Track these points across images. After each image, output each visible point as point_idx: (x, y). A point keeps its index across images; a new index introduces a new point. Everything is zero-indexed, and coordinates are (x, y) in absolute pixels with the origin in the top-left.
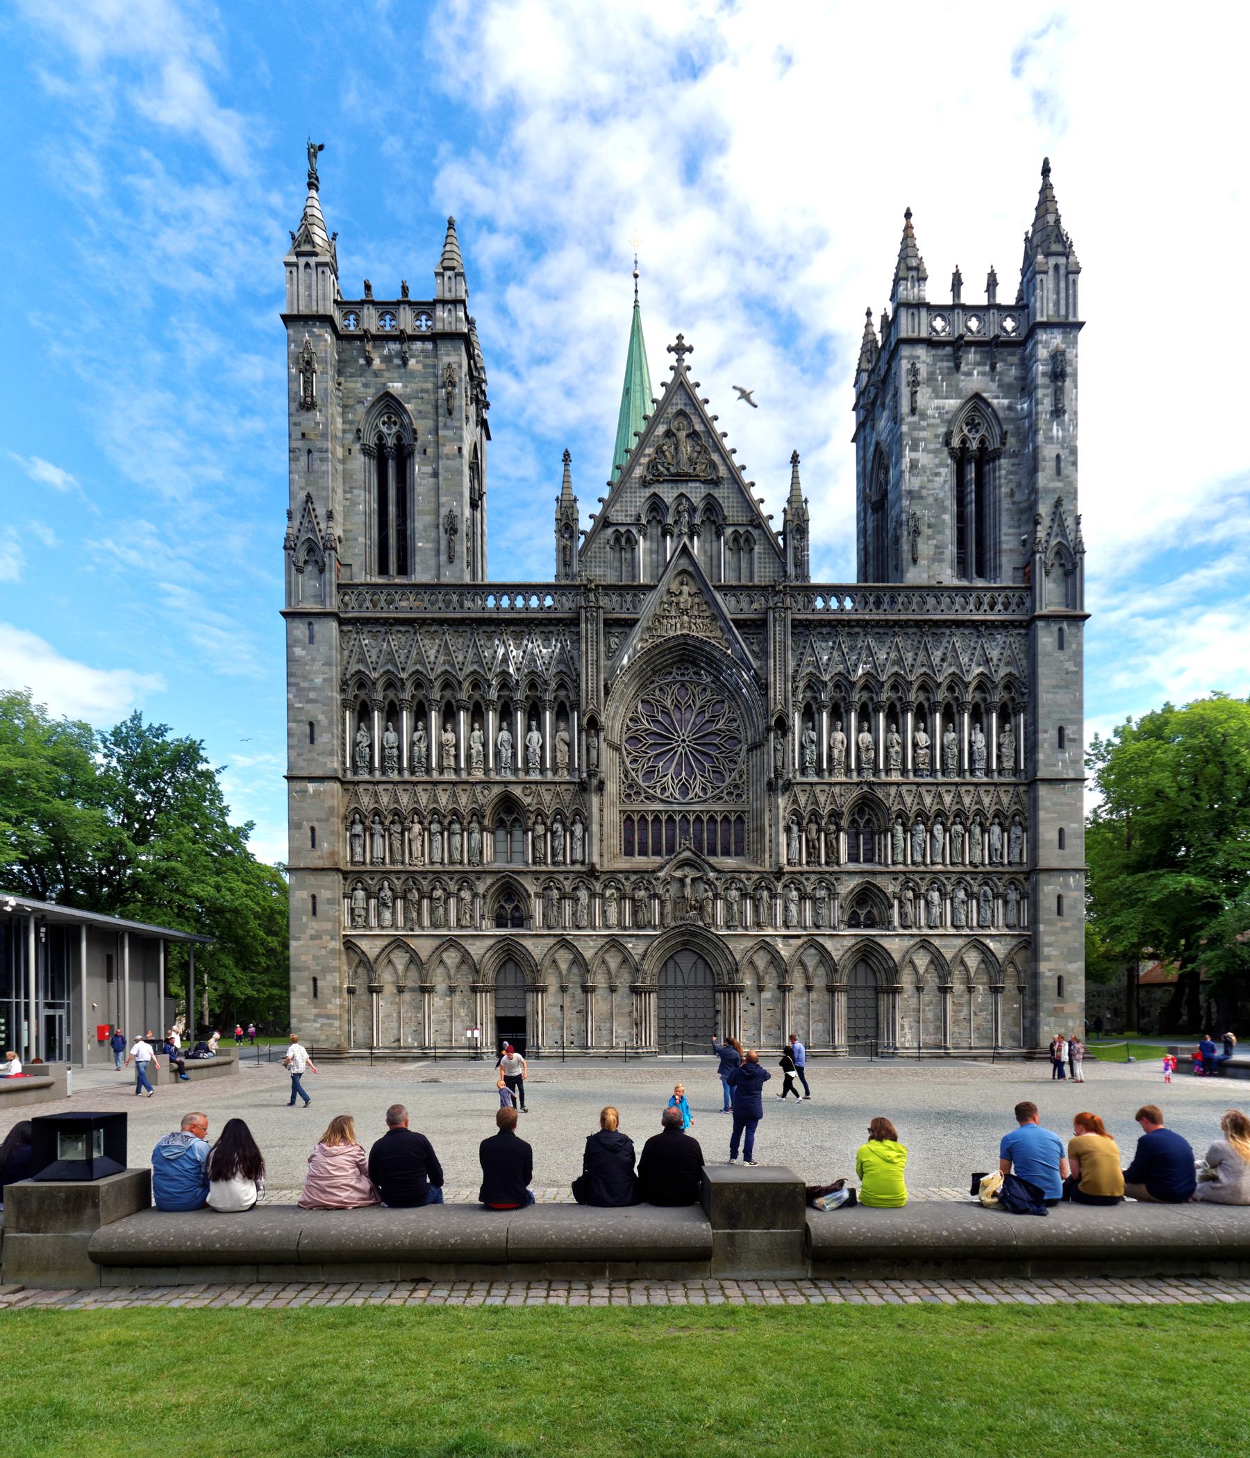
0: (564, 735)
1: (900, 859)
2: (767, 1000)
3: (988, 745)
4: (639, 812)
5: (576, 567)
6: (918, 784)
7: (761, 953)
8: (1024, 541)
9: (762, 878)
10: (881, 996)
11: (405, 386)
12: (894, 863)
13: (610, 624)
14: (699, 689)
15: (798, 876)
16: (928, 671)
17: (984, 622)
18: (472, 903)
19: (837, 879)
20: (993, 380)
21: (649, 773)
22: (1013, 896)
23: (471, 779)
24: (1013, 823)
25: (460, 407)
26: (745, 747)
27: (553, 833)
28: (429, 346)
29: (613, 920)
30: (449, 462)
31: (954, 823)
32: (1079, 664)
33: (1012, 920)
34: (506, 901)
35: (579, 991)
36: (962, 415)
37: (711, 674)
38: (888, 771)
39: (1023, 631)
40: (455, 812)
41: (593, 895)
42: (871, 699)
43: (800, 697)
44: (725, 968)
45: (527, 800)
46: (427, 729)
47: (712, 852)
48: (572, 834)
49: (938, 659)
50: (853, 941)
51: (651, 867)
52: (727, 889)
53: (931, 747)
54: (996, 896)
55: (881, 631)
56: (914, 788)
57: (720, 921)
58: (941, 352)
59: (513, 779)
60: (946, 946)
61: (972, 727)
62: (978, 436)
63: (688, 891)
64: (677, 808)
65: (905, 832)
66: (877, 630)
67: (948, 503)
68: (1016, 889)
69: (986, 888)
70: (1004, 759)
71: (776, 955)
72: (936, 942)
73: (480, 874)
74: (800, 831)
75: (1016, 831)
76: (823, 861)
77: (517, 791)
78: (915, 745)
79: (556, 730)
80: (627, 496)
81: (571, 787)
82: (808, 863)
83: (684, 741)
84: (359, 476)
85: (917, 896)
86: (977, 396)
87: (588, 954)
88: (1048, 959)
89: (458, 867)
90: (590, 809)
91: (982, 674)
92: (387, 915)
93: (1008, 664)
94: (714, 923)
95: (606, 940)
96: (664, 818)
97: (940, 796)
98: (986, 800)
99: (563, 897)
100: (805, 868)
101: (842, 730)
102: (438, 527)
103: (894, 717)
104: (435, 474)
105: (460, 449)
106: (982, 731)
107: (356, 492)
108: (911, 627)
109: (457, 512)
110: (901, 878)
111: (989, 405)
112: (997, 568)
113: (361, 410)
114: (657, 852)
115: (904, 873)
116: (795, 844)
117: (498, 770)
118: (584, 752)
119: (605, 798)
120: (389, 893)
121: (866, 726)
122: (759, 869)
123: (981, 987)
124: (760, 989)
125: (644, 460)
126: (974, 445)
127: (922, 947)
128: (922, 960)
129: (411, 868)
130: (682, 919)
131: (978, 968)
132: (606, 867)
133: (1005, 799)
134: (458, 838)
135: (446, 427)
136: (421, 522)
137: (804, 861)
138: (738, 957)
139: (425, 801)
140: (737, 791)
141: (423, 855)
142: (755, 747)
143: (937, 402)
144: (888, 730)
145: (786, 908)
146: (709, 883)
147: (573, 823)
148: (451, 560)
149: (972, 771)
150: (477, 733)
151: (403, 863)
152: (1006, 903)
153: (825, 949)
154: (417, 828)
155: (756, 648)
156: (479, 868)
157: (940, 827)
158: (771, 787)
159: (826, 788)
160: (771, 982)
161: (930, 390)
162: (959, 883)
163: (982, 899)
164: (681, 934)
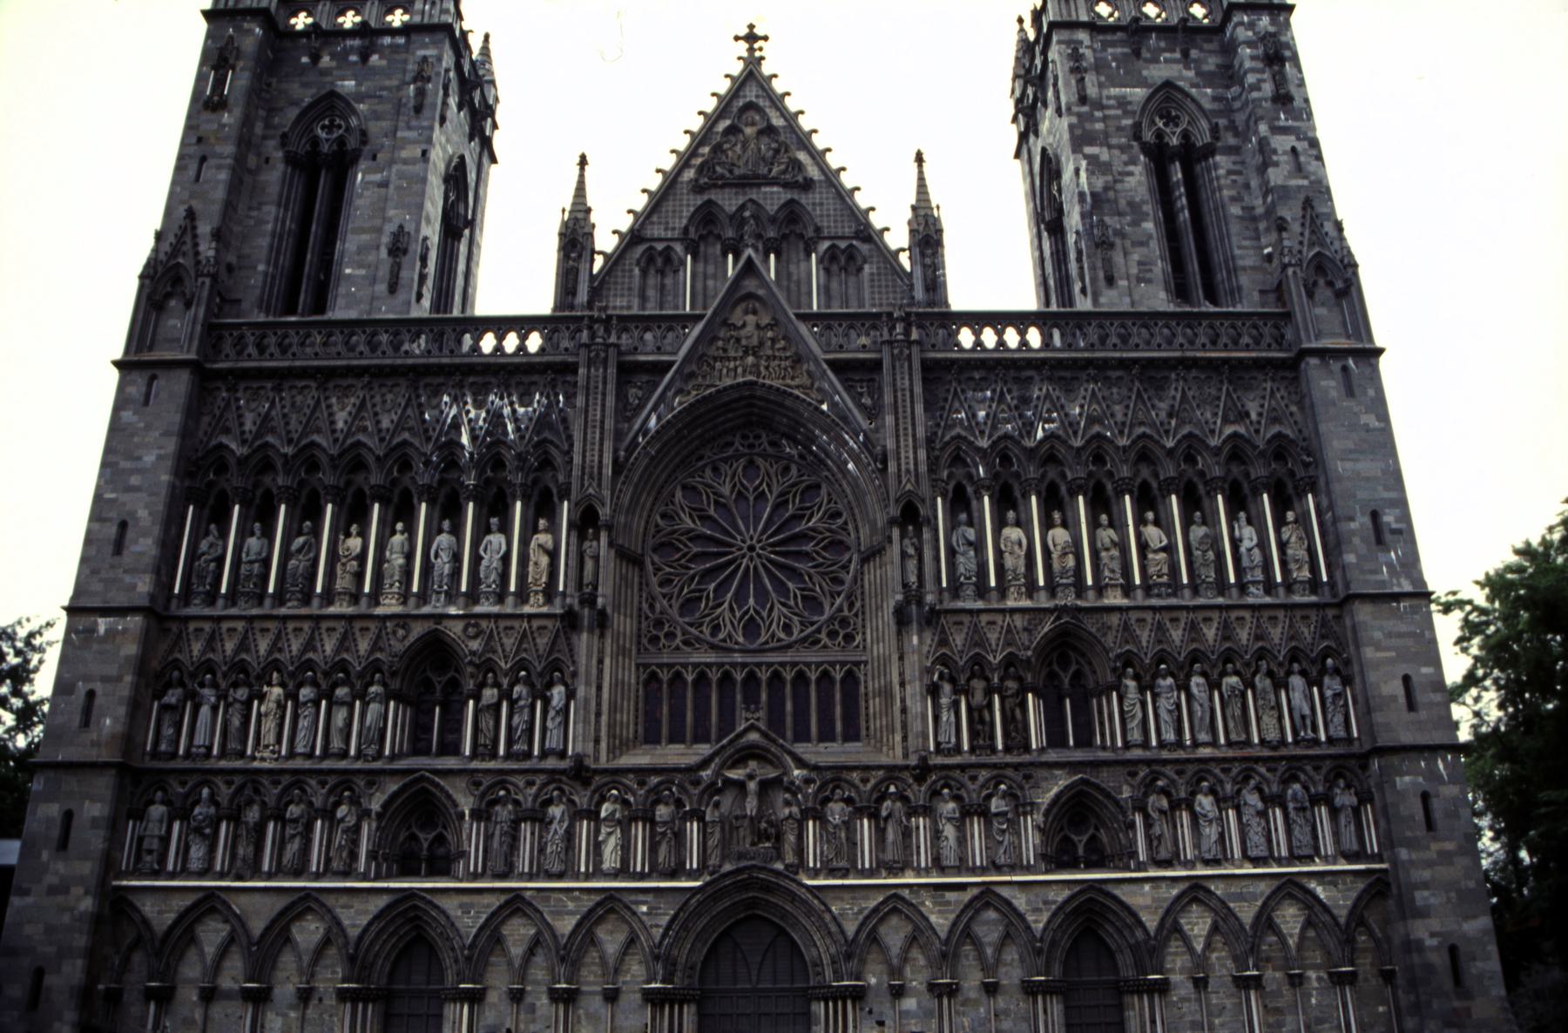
0: (544, 538)
1: (1136, 736)
2: (904, 1014)
3: (1263, 544)
5: (582, 296)
6: (1153, 609)
7: (894, 921)
8: (1270, 256)
10: (1127, 999)
11: (359, 84)
12: (1127, 745)
13: (628, 371)
15: (957, 774)
16: (1148, 431)
17: (1225, 361)
18: (357, 829)
19: (1027, 777)
20: (1187, 67)
21: (689, 605)
22: (1344, 799)
23: (379, 611)
24: (1323, 671)
25: (434, 105)
26: (855, 557)
27: (512, 703)
28: (401, 40)
29: (610, 859)
30: (404, 168)
31: (1224, 674)
32: (1384, 417)
33: (1350, 843)
34: (423, 827)
35: (545, 1000)
36: (1153, 105)
38: (1100, 589)
39: (1288, 374)
40: (343, 666)
41: (576, 815)
42: (1064, 476)
43: (945, 474)
45: (475, 645)
46: (317, 533)
47: (802, 735)
48: (547, 702)
49: (1163, 415)
50: (1066, 893)
52: (827, 800)
53: (1170, 549)
54: (1315, 800)
55: (1068, 374)
56: (1148, 616)
58: (1109, 37)
59: (453, 611)
60: (1240, 897)
61: (1232, 518)
62: (1178, 130)
65: (1142, 690)
66: (1063, 374)
67: (1148, 208)
68: (1348, 786)
69: (1297, 786)
70: (1293, 566)
71: (922, 924)
72: (1218, 889)
73: (373, 777)
74: (956, 692)
75: (1332, 684)
77: (456, 629)
78: (1143, 547)
79: (530, 529)
80: (669, 205)
81: (548, 623)
82: (972, 750)
83: (752, 548)
84: (273, 190)
85: (1175, 805)
86: (1168, 84)
88: (1423, 913)
89: (343, 764)
91: (1235, 435)
92: (197, 852)
93: (1275, 420)
95: (597, 898)
96: (714, 676)
97: (1193, 627)
98: (1276, 633)
101: (1018, 524)
102: (378, 248)
103: (1101, 504)
104: (384, 184)
105: (424, 153)
106: (1249, 522)
107: (266, 208)
108: (1114, 368)
109: (410, 227)
110: (1143, 772)
111: (1187, 95)
112: (1235, 293)
113: (293, 113)
115: (1148, 762)
117: (423, 597)
118: (572, 563)
119: (608, 641)
120: (212, 810)
121: (1057, 516)
122: (884, 760)
123: (1312, 974)
124: (898, 992)
125: (698, 161)
126: (1175, 141)
127: (1196, 900)
128: (1197, 924)
129: (256, 764)
130: (741, 856)
131: (1302, 936)
132: (603, 763)
133: (1306, 632)
134: (340, 716)
135: (409, 128)
136: (350, 243)
137: (966, 747)
139: (294, 649)
140: (844, 629)
141: (279, 741)
142: (872, 555)
143: (1114, 91)
144: (1094, 525)
145: (937, 835)
146: (792, 789)
147: (550, 685)
148: (393, 288)
149: (1242, 587)
150: (398, 539)
151: (241, 754)
152: (1334, 813)
153: (1014, 910)
154: (277, 692)
155: (867, 401)
156: (378, 765)
157: (1201, 680)
159: (999, 618)
160: (916, 979)
161: (1103, 79)
162: (1247, 778)
163: (1291, 806)
164: (745, 886)
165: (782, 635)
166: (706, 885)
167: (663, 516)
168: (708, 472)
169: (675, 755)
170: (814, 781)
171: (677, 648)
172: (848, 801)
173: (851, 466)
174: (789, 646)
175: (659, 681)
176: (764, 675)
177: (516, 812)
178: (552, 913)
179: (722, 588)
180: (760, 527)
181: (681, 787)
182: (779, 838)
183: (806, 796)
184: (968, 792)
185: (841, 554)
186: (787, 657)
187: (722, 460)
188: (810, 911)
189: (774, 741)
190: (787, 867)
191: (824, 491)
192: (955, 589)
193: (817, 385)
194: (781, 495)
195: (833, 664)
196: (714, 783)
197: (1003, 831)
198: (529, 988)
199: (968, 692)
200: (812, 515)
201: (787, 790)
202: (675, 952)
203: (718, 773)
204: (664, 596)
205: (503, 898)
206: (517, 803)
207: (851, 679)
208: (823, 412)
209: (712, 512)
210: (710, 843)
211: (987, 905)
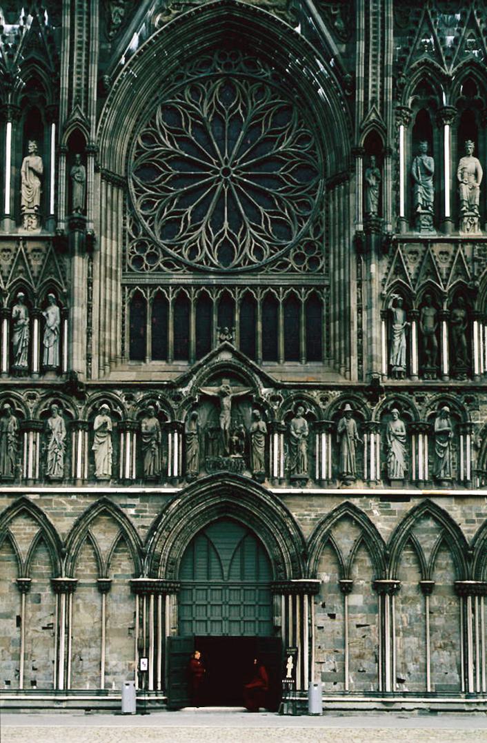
4: (154, 286)
9: (345, 399)
14: (254, 88)
15: (405, 395)
19: (469, 400)
21: (170, 228)
26: (322, 181)
29: (104, 467)
37: (271, 64)
41: (73, 426)
44: (285, 550)
51: (166, 378)
57: (278, 470)
63: (225, 421)
64: (213, 279)
74: (408, 318)
76: (446, 371)
82: (421, 373)
83: (226, 172)
87: (63, 526)
90: (70, 285)
94: (268, 473)
95: (92, 501)
96: (193, 296)
99: (25, 426)
100: (417, 381)
114: (182, 354)
116: (399, 341)
122: (342, 381)
130: (217, 465)
137: (415, 370)
138: (307, 531)
146: (259, 405)
158: (362, 249)
165: (253, 259)
166: (186, 490)
167: (144, 138)
168: (187, 93)
169: (155, 370)
170: (279, 399)
171: (159, 269)
172: (309, 417)
173: (321, 91)
174: (260, 269)
175: (144, 301)
176: (237, 297)
177: (20, 424)
178: (53, 514)
179: (197, 216)
180: (234, 153)
181: (163, 401)
182: (248, 451)
183: (272, 412)
184: (415, 412)
185: (309, 179)
186: (257, 280)
187: (203, 80)
188: (273, 515)
189: (245, 362)
190: (254, 475)
191: (295, 114)
192: (413, 220)
193: (293, 5)
194: (253, 119)
195: (298, 287)
196: (192, 399)
197: (445, 449)
198: (35, 581)
199: (420, 319)
200: (282, 140)
201: (256, 406)
202: (158, 550)
203: (195, 390)
204: (146, 218)
205: (12, 500)
206: (18, 414)
207: (314, 301)
208: (297, 34)
209: (189, 134)
210: (189, 453)
211: (427, 515)
